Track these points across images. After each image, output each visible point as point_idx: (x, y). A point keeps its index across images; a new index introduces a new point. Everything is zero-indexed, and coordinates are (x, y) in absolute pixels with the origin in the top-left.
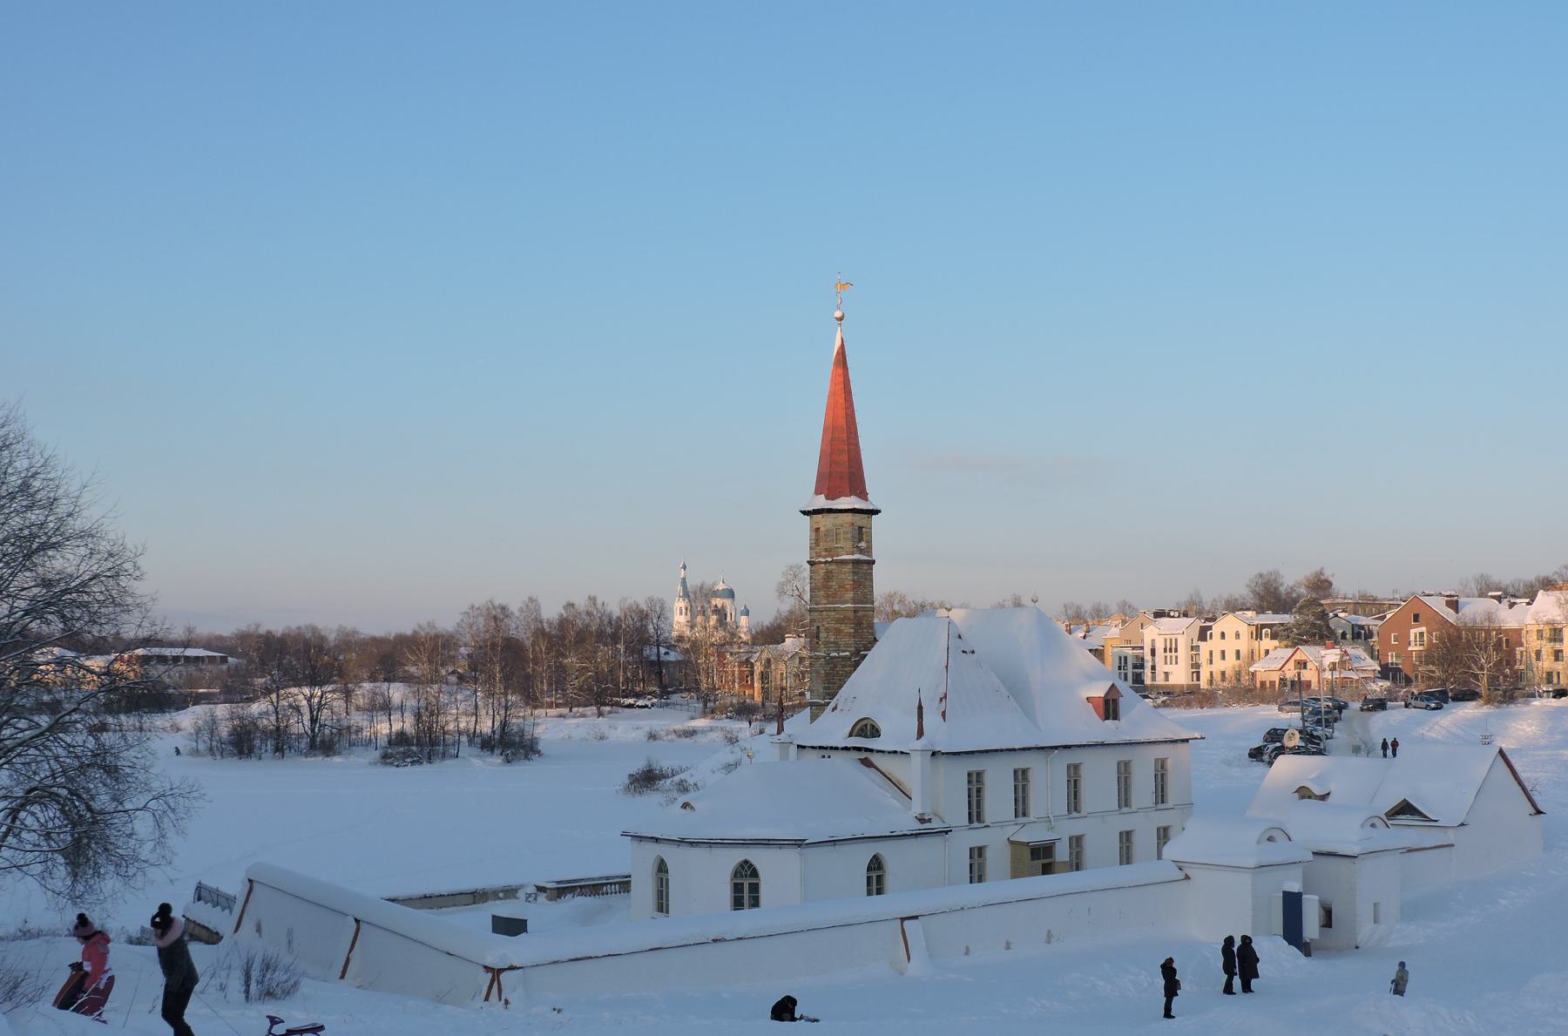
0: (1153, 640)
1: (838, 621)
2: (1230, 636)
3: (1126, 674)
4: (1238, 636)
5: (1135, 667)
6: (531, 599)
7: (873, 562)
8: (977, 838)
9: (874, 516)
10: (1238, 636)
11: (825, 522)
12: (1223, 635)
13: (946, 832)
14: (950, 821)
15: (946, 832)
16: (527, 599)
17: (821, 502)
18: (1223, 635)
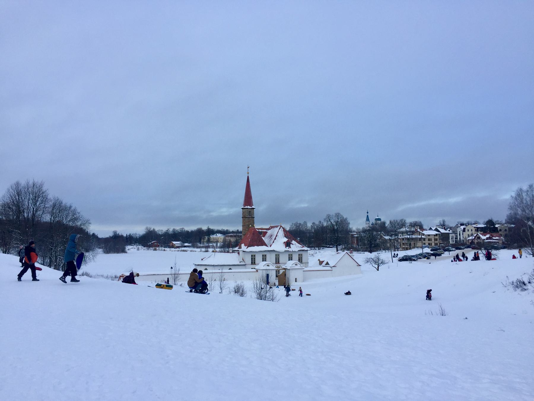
0: (460, 232)
1: (246, 228)
2: (470, 230)
3: (453, 241)
4: (472, 230)
5: (455, 239)
6: (305, 222)
7: (254, 217)
8: (253, 266)
9: (254, 209)
10: (472, 230)
11: (244, 210)
12: (468, 230)
13: (245, 265)
14: (246, 263)
15: (245, 265)
16: (304, 222)
17: (243, 207)
18: (468, 230)
